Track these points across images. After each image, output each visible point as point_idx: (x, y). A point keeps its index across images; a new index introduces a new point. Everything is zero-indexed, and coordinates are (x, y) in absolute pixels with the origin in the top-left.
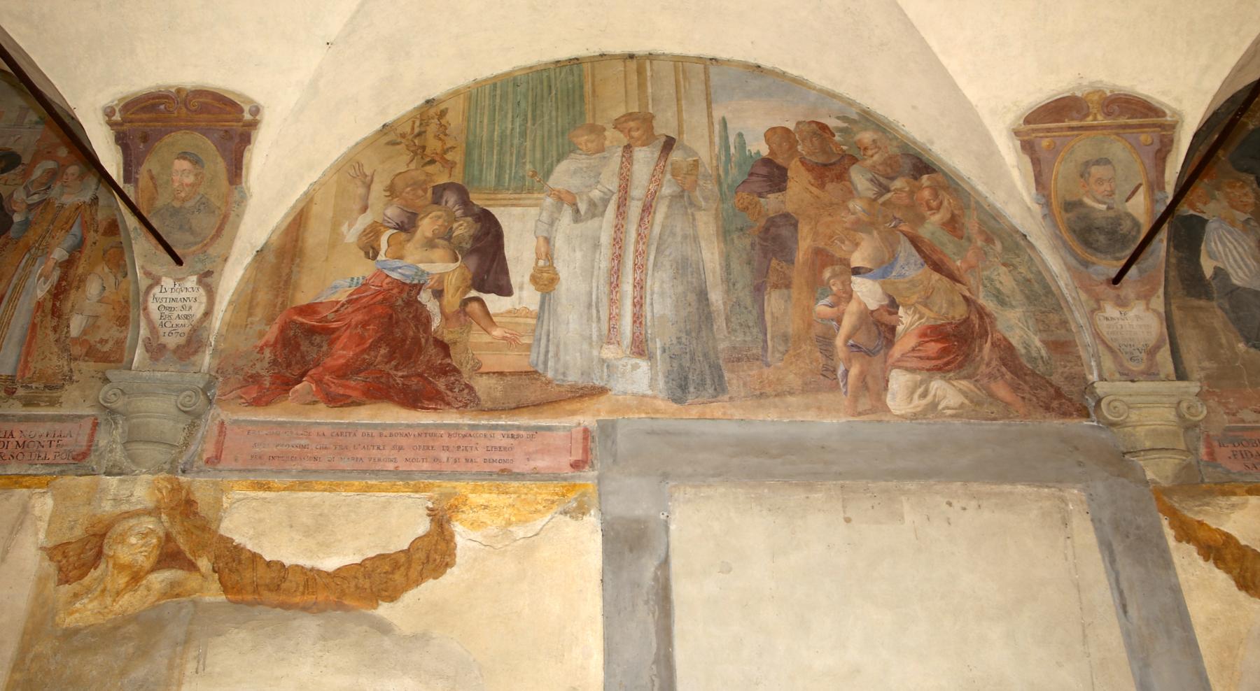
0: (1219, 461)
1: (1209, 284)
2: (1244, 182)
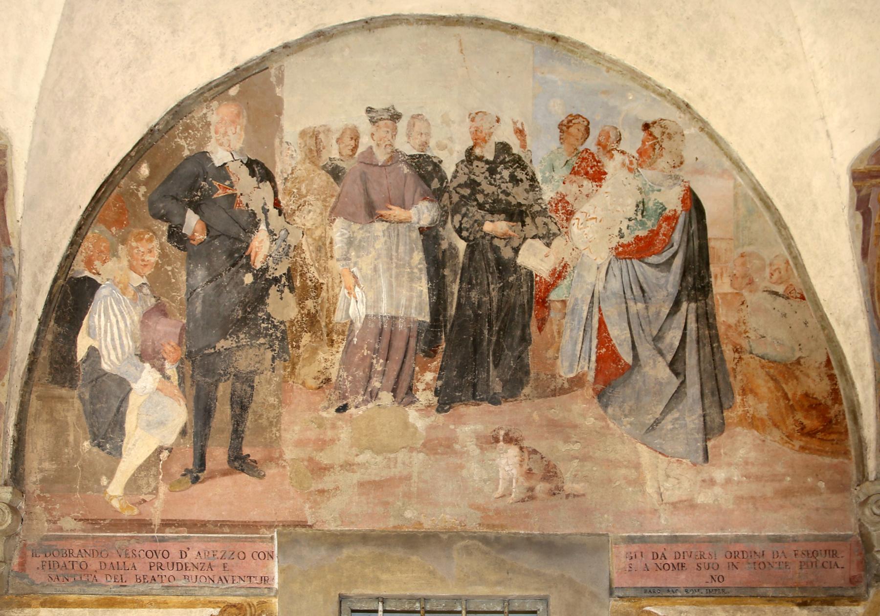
0: (28, 572)
1: (78, 368)
2: (154, 233)
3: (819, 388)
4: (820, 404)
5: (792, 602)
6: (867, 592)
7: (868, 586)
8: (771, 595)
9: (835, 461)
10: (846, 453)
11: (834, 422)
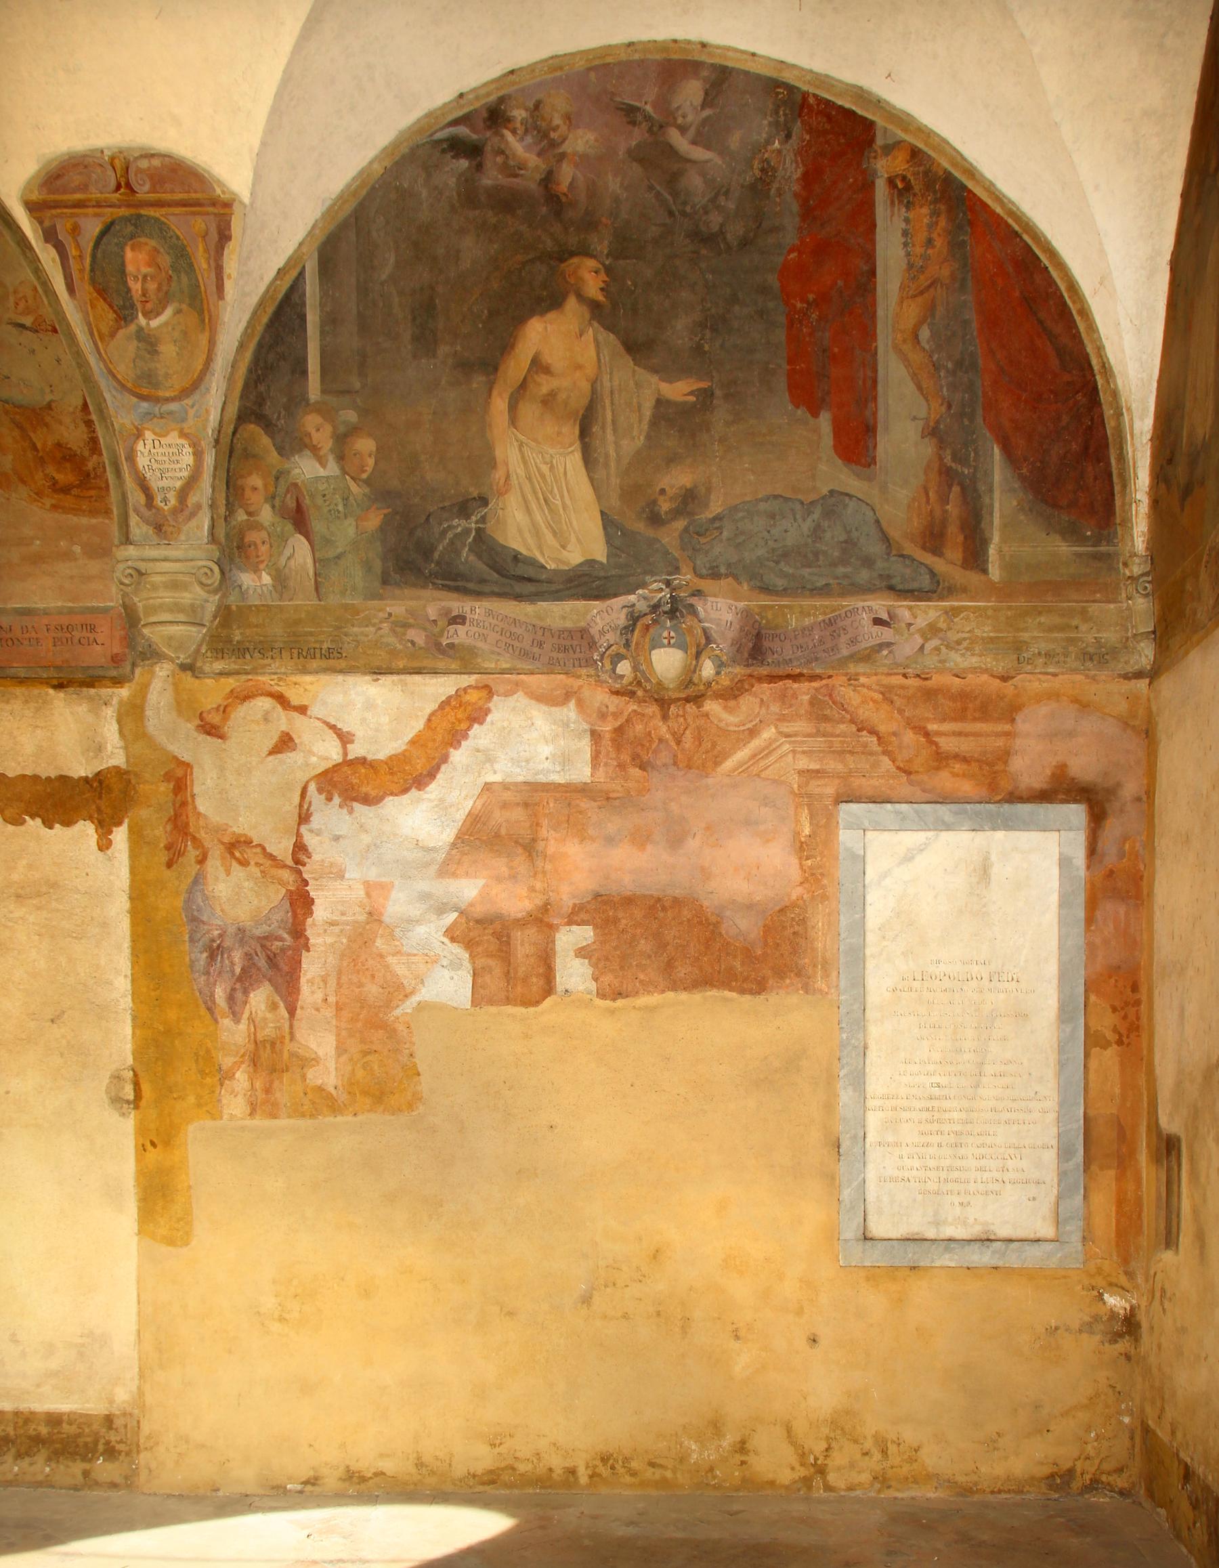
3: (74, 436)
4: (75, 455)
5: (47, 683)
6: (133, 673)
7: (134, 665)
8: (23, 675)
9: (94, 521)
10: (107, 512)
11: (92, 476)
